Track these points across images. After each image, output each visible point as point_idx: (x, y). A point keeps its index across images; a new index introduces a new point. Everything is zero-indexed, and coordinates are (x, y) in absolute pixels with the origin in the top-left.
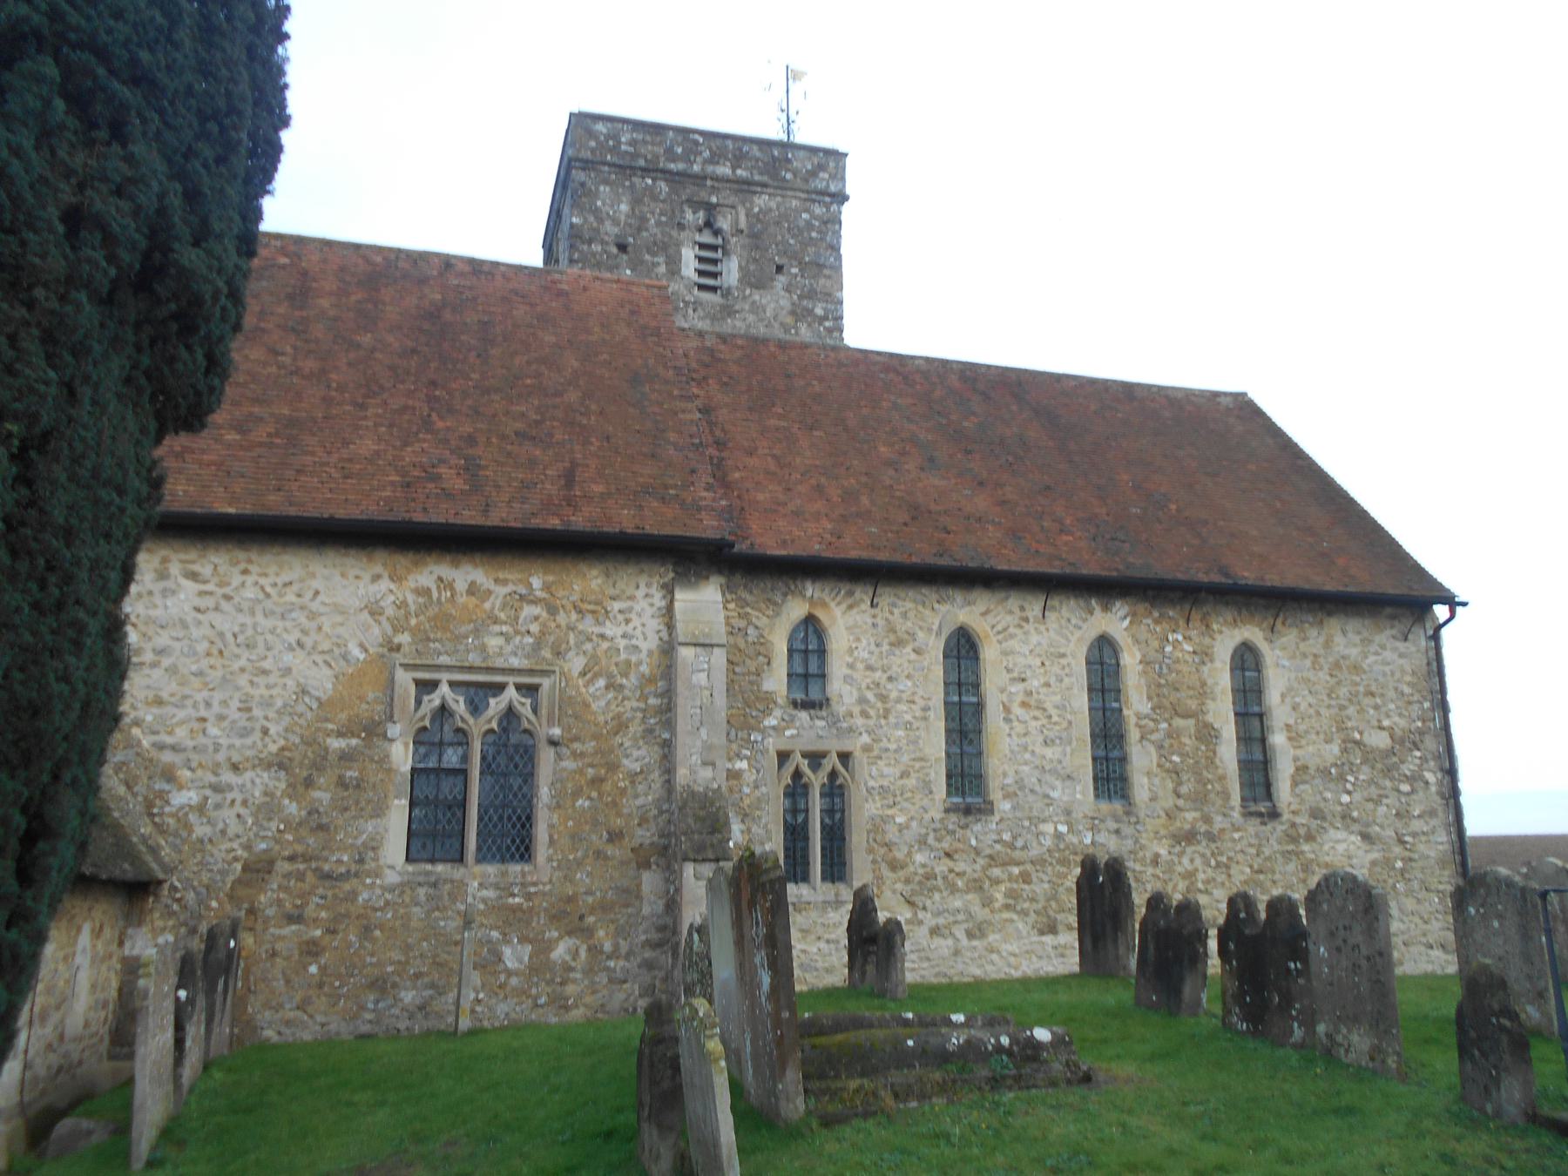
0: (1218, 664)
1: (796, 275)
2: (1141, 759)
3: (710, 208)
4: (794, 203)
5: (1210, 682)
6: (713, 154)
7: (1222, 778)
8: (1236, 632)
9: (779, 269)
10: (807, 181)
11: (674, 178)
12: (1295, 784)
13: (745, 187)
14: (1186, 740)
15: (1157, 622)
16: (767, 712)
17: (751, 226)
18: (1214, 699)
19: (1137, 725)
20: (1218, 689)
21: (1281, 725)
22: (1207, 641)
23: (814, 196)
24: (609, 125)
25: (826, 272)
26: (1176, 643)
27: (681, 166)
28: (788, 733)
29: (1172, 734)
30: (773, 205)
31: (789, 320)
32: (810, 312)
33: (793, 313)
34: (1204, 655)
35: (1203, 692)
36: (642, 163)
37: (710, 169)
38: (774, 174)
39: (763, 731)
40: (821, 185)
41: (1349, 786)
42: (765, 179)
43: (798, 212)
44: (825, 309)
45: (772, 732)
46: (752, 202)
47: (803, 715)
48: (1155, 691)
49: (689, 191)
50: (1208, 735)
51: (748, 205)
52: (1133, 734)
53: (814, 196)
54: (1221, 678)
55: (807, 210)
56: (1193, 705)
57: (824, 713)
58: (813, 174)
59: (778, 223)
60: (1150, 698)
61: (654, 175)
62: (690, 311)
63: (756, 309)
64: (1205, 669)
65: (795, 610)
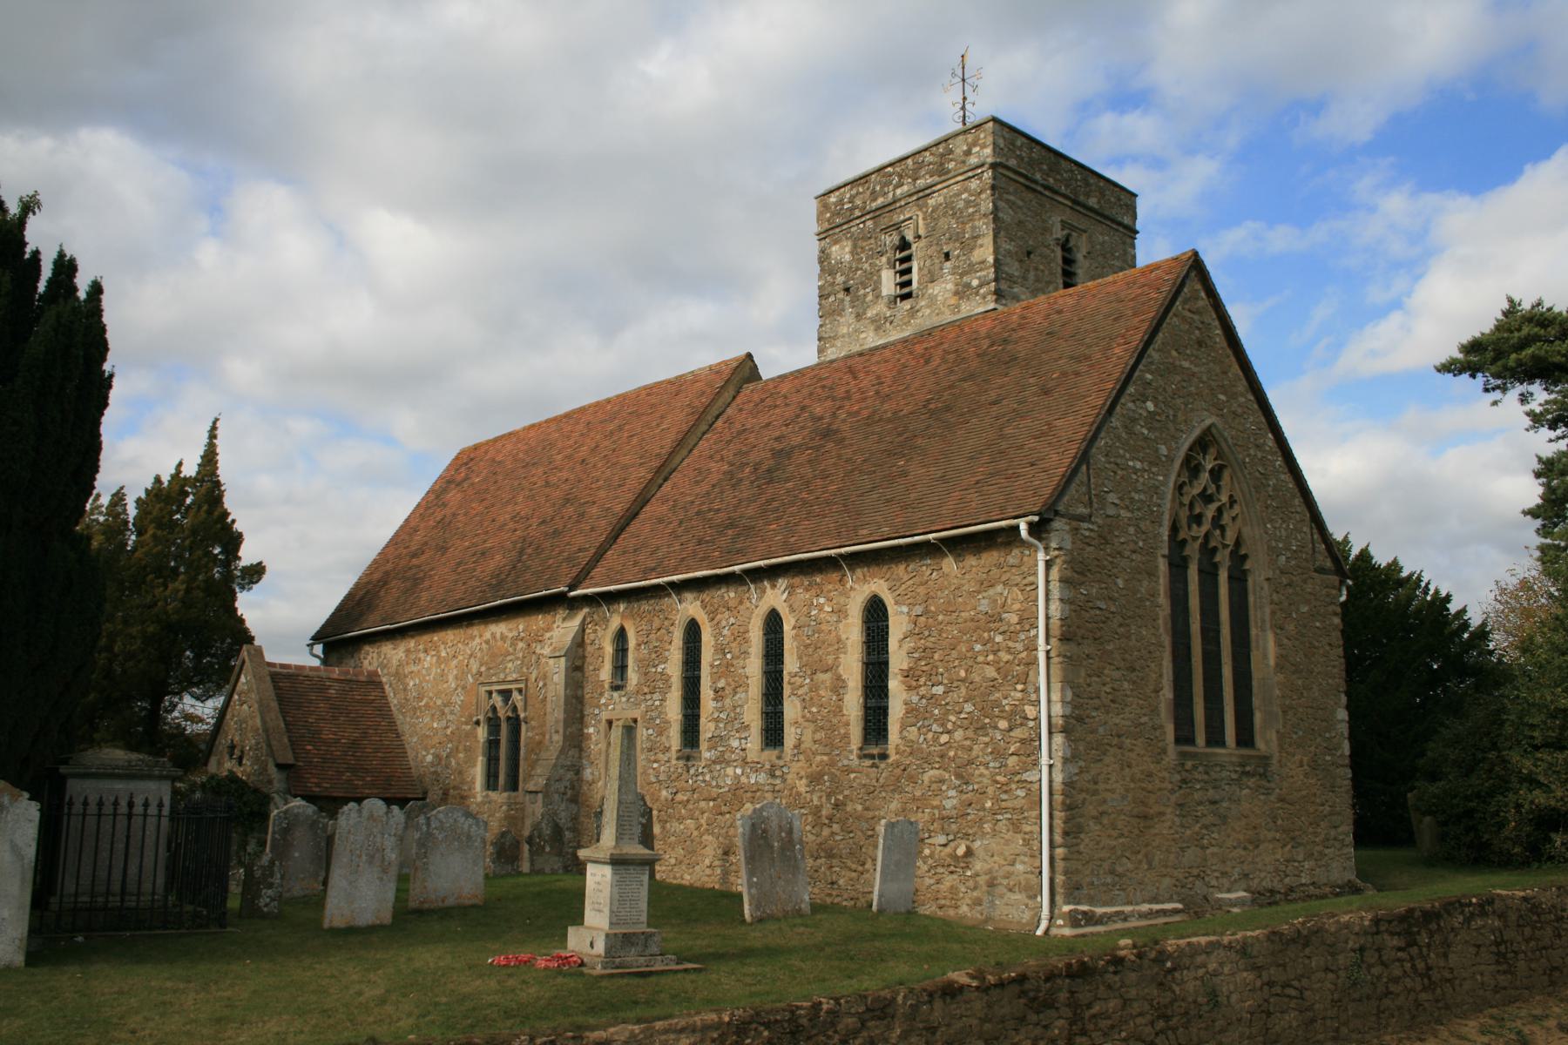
0: (850, 620)
1: (958, 256)
2: (791, 709)
3: (897, 227)
4: (956, 187)
5: (844, 637)
6: (901, 177)
7: (848, 724)
8: (866, 586)
9: (947, 256)
10: (964, 162)
11: (877, 213)
12: (903, 728)
13: (921, 194)
14: (822, 693)
15: (807, 590)
16: (601, 694)
17: (927, 225)
18: (845, 653)
19: (789, 683)
20: (849, 643)
21: (896, 671)
22: (842, 600)
23: (970, 174)
24: (837, 193)
25: (980, 242)
26: (820, 608)
27: (880, 201)
28: (610, 708)
29: (814, 688)
30: (941, 199)
31: (953, 301)
32: (968, 286)
33: (956, 293)
34: (841, 612)
35: (840, 647)
36: (857, 213)
37: (899, 191)
38: (941, 171)
39: (598, 706)
40: (973, 160)
41: (950, 726)
42: (936, 179)
43: (959, 194)
44: (979, 278)
45: (603, 708)
46: (926, 205)
47: (616, 694)
48: (805, 649)
49: (885, 221)
50: (839, 686)
51: (924, 210)
52: (787, 690)
53: (970, 174)
54: (853, 632)
55: (966, 190)
56: (830, 659)
57: (623, 693)
58: (968, 153)
59: (945, 214)
60: (800, 658)
61: (863, 219)
62: (888, 324)
63: (933, 299)
64: (841, 626)
65: (615, 623)
